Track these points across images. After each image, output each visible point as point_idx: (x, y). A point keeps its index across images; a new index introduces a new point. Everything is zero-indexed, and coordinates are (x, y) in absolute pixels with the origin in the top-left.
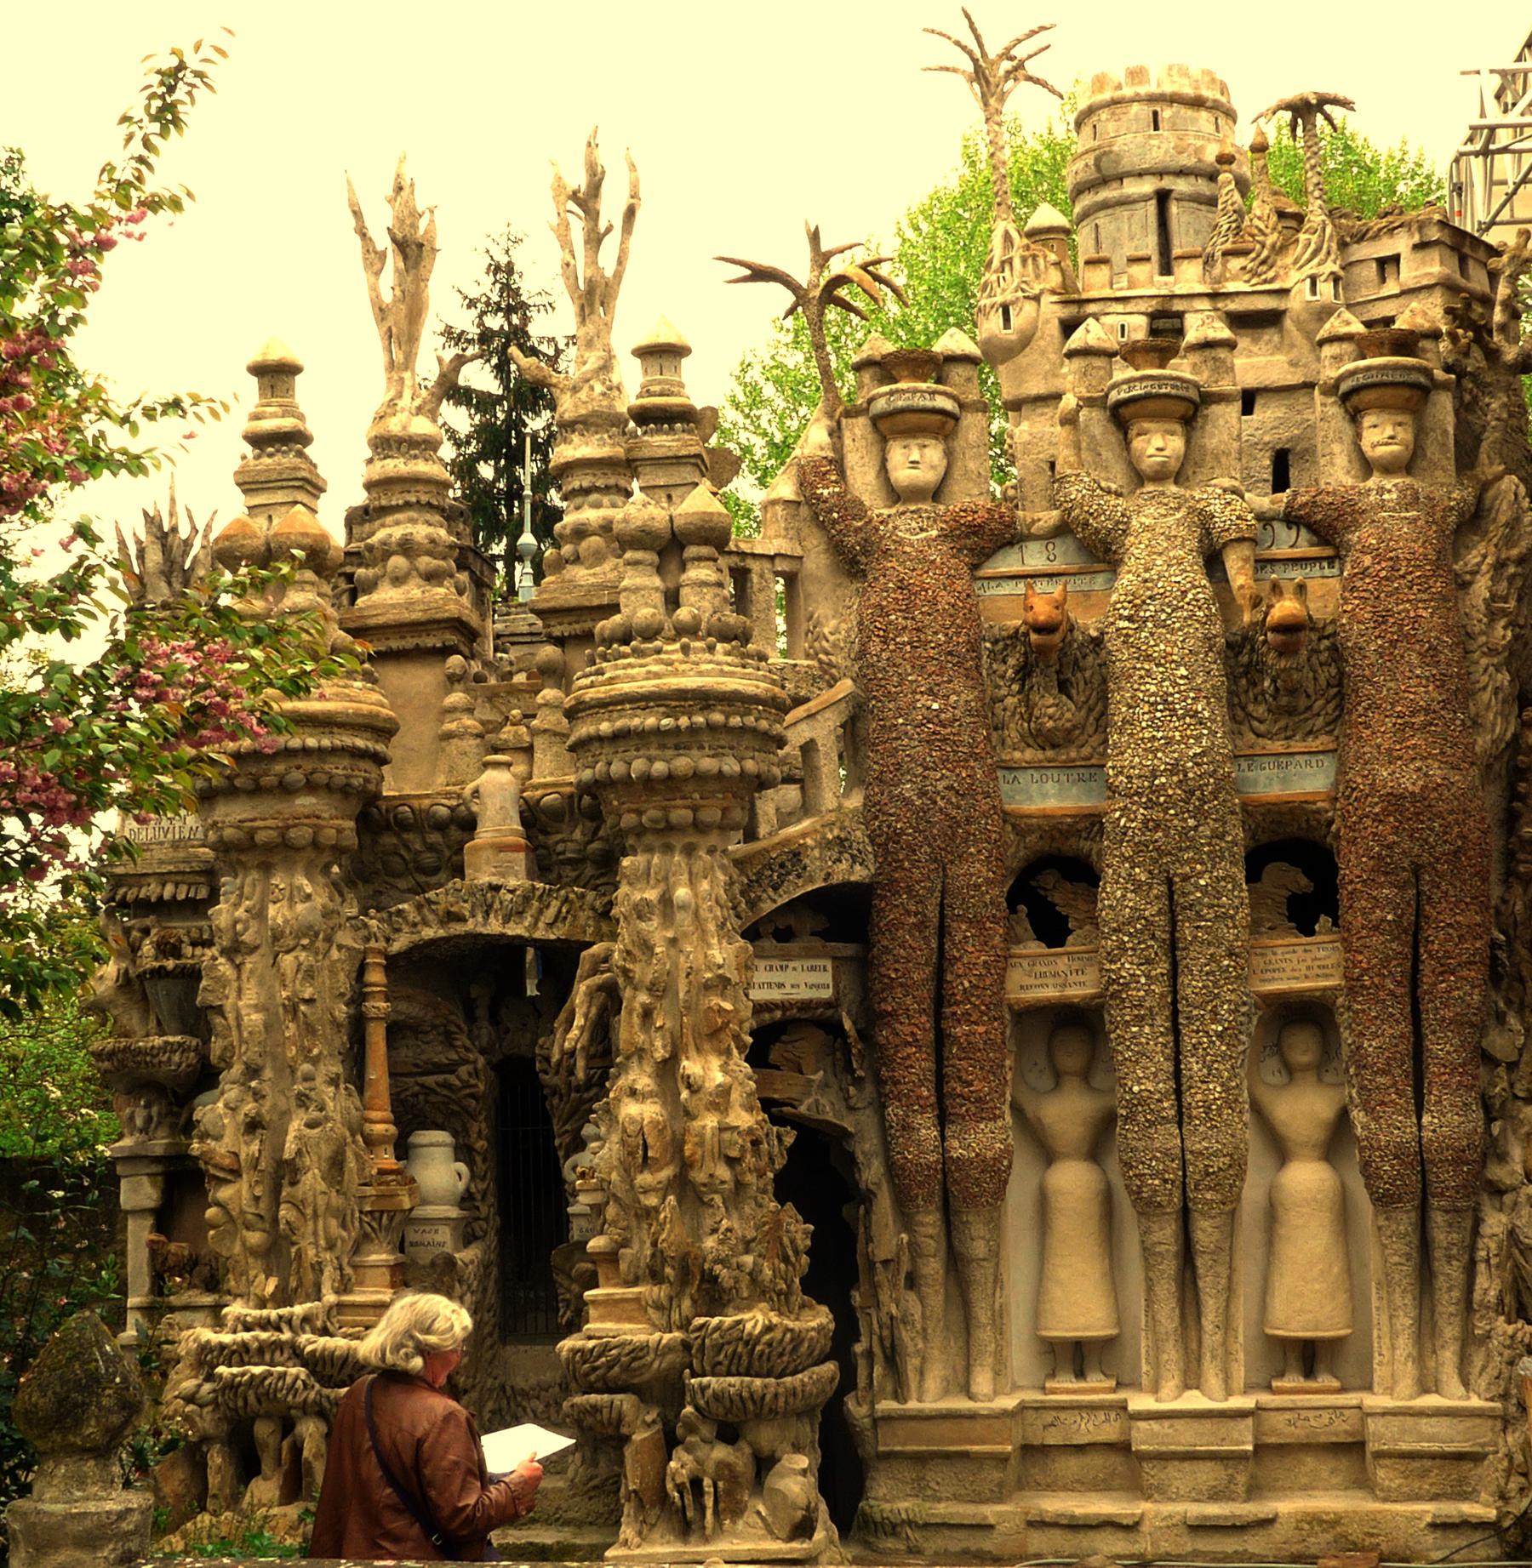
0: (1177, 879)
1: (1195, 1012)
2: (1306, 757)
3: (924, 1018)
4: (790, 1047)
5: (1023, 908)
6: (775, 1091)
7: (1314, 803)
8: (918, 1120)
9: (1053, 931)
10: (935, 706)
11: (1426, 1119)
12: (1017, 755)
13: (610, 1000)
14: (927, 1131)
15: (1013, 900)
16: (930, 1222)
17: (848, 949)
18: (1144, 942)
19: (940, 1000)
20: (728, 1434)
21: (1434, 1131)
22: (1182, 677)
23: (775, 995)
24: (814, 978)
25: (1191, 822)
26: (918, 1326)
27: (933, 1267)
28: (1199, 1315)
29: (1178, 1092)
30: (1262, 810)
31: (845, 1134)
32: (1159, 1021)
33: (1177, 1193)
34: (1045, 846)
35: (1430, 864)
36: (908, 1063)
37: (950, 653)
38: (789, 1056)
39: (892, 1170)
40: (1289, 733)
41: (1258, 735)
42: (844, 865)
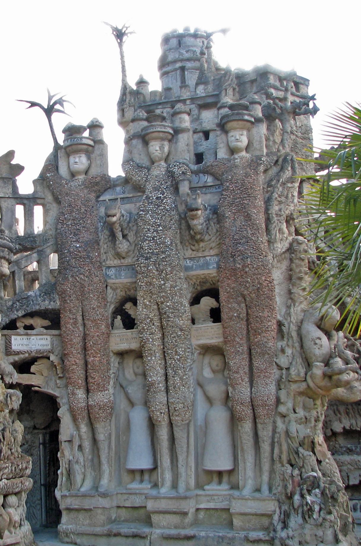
0: (159, 303)
1: (169, 351)
2: (210, 258)
3: (79, 355)
4: (37, 366)
5: (119, 317)
6: (33, 382)
7: (212, 274)
10: (78, 246)
11: (253, 389)
12: (111, 262)
14: (81, 394)
16: (84, 428)
18: (151, 326)
19: (85, 348)
21: (255, 394)
22: (161, 230)
24: (44, 342)
25: (162, 282)
26: (82, 464)
27: (87, 445)
28: (177, 461)
29: (166, 380)
30: (195, 277)
32: (158, 355)
33: (166, 418)
34: (123, 294)
35: (248, 294)
36: (74, 371)
37: (84, 227)
38: (38, 369)
40: (204, 249)
41: (193, 250)
42: (47, 302)
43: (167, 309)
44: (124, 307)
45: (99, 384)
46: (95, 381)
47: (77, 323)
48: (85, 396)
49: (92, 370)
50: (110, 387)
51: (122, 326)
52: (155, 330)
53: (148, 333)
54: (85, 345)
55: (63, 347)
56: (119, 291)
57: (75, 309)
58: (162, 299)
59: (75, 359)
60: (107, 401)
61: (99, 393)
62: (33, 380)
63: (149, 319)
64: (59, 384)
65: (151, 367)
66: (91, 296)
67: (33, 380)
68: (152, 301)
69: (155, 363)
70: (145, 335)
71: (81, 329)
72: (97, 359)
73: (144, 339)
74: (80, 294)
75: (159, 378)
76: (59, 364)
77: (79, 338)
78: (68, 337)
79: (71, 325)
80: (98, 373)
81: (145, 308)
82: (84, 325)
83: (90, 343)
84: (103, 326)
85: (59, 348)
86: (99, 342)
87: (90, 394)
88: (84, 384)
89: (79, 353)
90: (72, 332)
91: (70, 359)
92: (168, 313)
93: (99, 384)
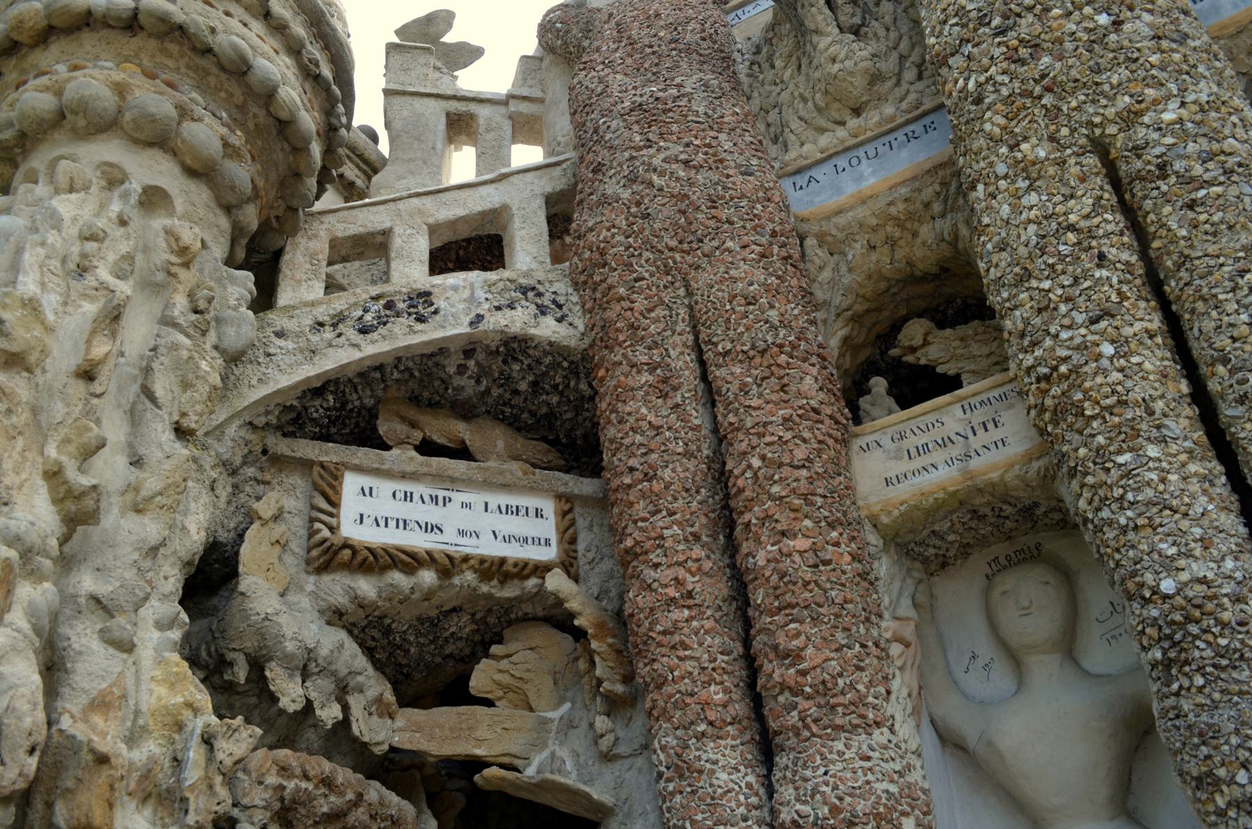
3: (698, 552)
4: (504, 664)
6: (480, 742)
8: (710, 751)
25: (1103, 19)
43: (1169, 140)
44: (894, 352)
45: (824, 689)
46: (803, 673)
47: (675, 389)
48: (751, 779)
49: (780, 609)
50: (896, 708)
51: (895, 406)
52: (1120, 293)
53: (1080, 318)
54: (726, 507)
55: (612, 529)
56: (856, 250)
57: (657, 320)
58: (1127, 99)
59: (681, 573)
60: (893, 789)
61: (839, 745)
62: (482, 733)
63: (1071, 237)
64: (609, 738)
65: (1150, 503)
66: (730, 244)
67: (478, 734)
68: (1065, 131)
69: (1173, 477)
70: (1064, 335)
71: (698, 416)
72: (801, 543)
73: (1065, 360)
74: (673, 243)
75: (1229, 564)
76: (601, 626)
77: (691, 465)
78: (633, 462)
79: (646, 402)
80: (815, 620)
81: (1030, 188)
82: (710, 394)
83: (749, 466)
84: (809, 380)
85: (607, 565)
86: (800, 454)
87: (782, 760)
88: (740, 708)
89: (697, 537)
90: (651, 433)
91: (649, 574)
92: (1178, 166)
93: (824, 689)
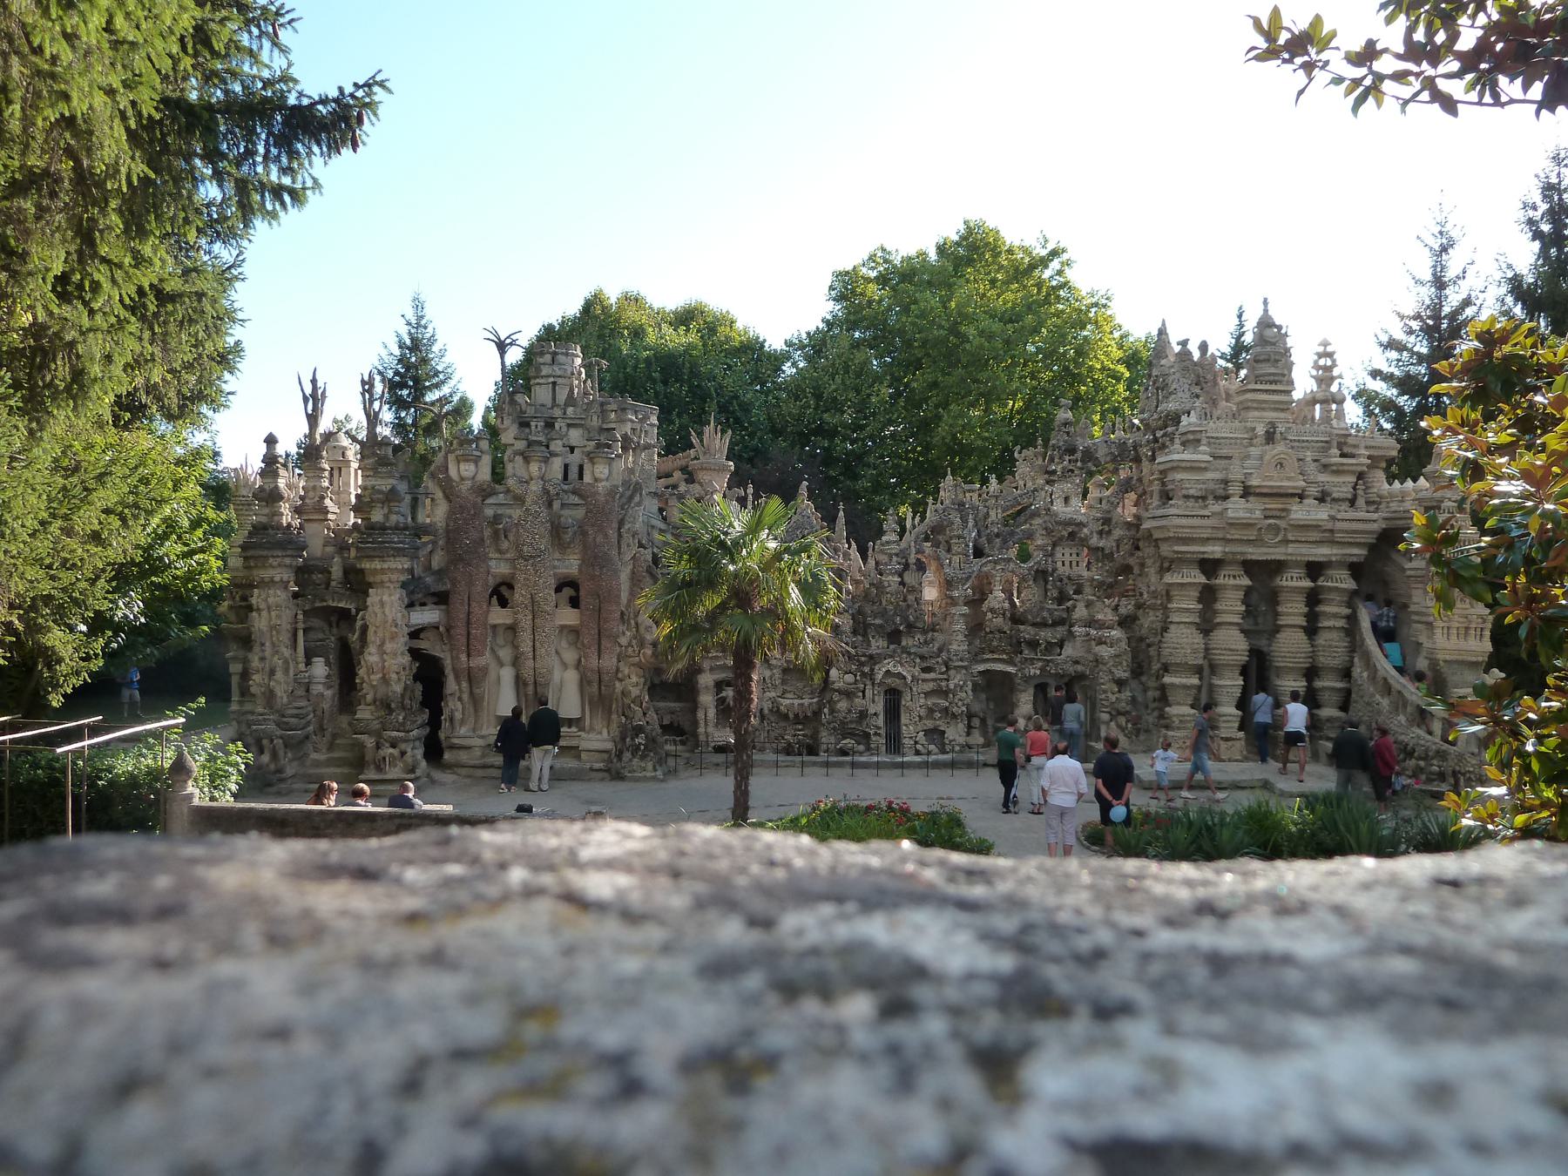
9: (503, 603)
13: (365, 629)
14: (463, 657)
15: (491, 596)
16: (465, 685)
17: (443, 607)
19: (468, 623)
20: (393, 746)
23: (420, 621)
31: (440, 659)
39: (454, 669)
